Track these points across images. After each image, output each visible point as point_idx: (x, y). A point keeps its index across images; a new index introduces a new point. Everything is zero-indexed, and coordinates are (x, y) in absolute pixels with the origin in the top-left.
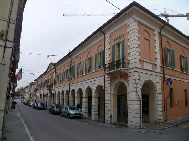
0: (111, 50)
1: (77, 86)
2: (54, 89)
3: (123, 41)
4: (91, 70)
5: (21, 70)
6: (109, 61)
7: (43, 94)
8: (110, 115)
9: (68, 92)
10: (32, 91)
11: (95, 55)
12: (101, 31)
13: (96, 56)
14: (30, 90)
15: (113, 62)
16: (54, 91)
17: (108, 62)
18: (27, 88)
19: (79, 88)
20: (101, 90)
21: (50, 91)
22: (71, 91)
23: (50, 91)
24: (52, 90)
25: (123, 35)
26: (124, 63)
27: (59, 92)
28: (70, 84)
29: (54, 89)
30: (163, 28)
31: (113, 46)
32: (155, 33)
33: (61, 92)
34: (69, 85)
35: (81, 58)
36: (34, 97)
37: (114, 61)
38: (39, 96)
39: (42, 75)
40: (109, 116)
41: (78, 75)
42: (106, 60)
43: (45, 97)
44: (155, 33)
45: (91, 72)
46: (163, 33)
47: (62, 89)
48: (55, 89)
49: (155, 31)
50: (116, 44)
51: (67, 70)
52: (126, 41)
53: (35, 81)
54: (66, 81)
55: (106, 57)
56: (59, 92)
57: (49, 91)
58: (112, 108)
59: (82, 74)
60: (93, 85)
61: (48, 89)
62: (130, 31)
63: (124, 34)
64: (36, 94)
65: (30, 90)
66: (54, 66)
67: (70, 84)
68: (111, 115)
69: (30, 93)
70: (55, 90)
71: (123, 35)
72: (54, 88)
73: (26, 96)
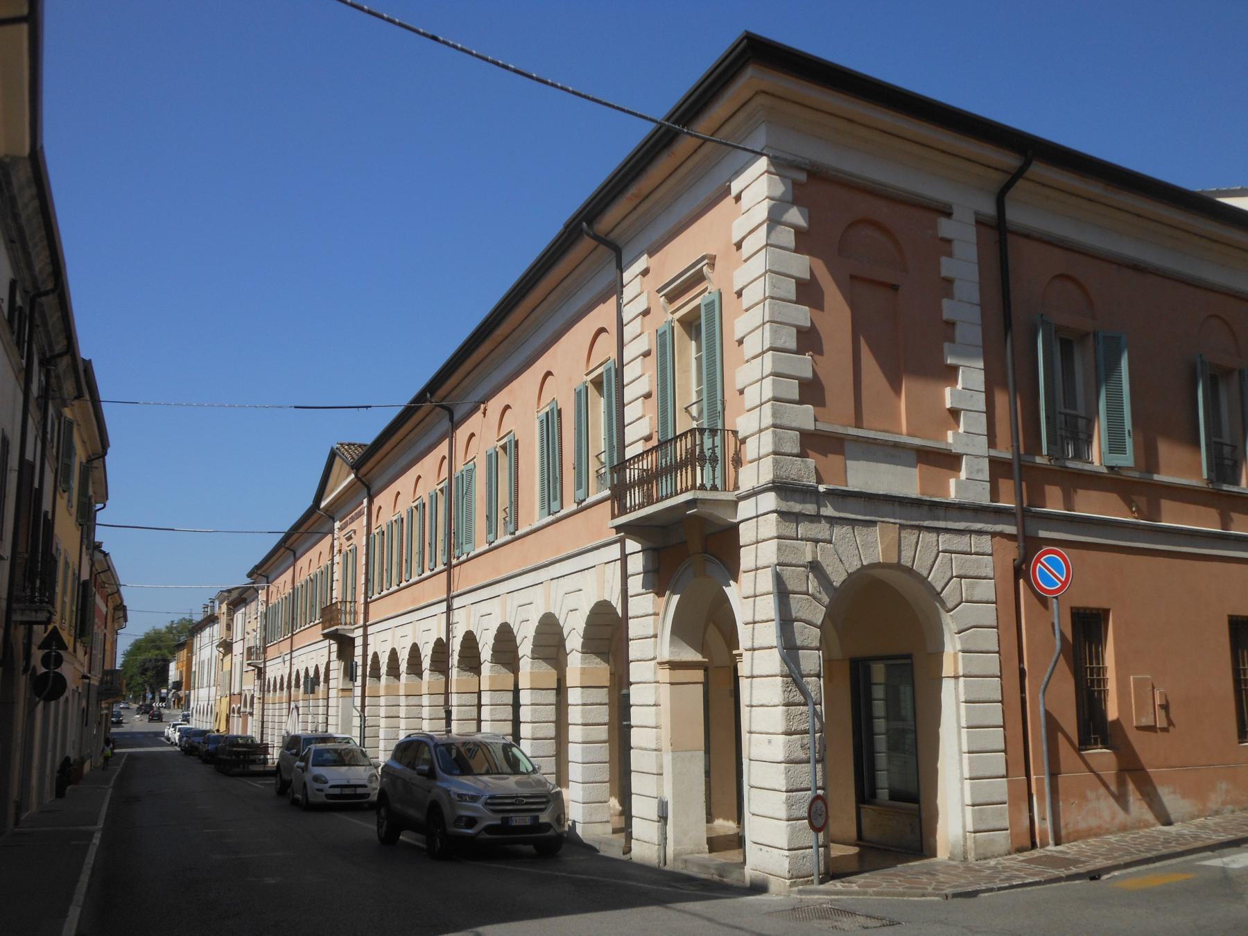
0: (652, 360)
1: (484, 608)
2: (365, 636)
3: (710, 305)
4: (555, 499)
5: (65, 550)
6: (648, 439)
7: (302, 674)
8: (655, 803)
9: (441, 648)
10: (238, 648)
11: (572, 397)
12: (596, 237)
13: (581, 398)
14: (227, 647)
15: (662, 444)
16: (365, 645)
17: (638, 448)
18: (208, 631)
19: (467, 632)
20: (1126, 454)
21: (345, 645)
22: (456, 645)
23: (345, 645)
24: (353, 640)
25: (711, 261)
26: (714, 460)
27: (394, 655)
28: (449, 600)
29: (365, 636)
30: (1020, 183)
31: (661, 336)
32: (946, 228)
33: (404, 657)
34: (443, 606)
35: (508, 411)
36: (253, 697)
37: (670, 436)
38: (281, 688)
39: (288, 536)
40: (654, 814)
41: (490, 532)
42: (631, 434)
43: (313, 692)
44: (946, 228)
45: (558, 515)
46: (1016, 216)
47: (408, 630)
48: (370, 630)
49: (949, 215)
50: (676, 325)
51: (434, 498)
52: (729, 298)
53: (250, 575)
54: (376, 596)
55: (630, 413)
56: (394, 655)
57: (334, 647)
58: (667, 758)
59: (511, 528)
60: (571, 601)
61: (326, 636)
62: (744, 238)
63: (713, 258)
64: (261, 673)
65: (227, 647)
66: (356, 467)
67: (449, 600)
68: (663, 806)
69: (227, 667)
70: (370, 639)
71: (711, 261)
72: (365, 627)
73: (203, 693)
